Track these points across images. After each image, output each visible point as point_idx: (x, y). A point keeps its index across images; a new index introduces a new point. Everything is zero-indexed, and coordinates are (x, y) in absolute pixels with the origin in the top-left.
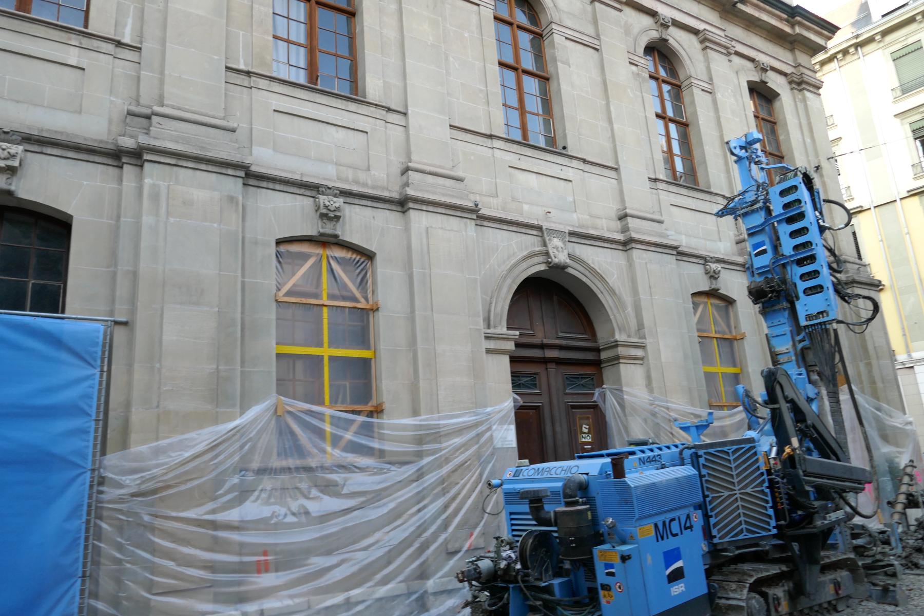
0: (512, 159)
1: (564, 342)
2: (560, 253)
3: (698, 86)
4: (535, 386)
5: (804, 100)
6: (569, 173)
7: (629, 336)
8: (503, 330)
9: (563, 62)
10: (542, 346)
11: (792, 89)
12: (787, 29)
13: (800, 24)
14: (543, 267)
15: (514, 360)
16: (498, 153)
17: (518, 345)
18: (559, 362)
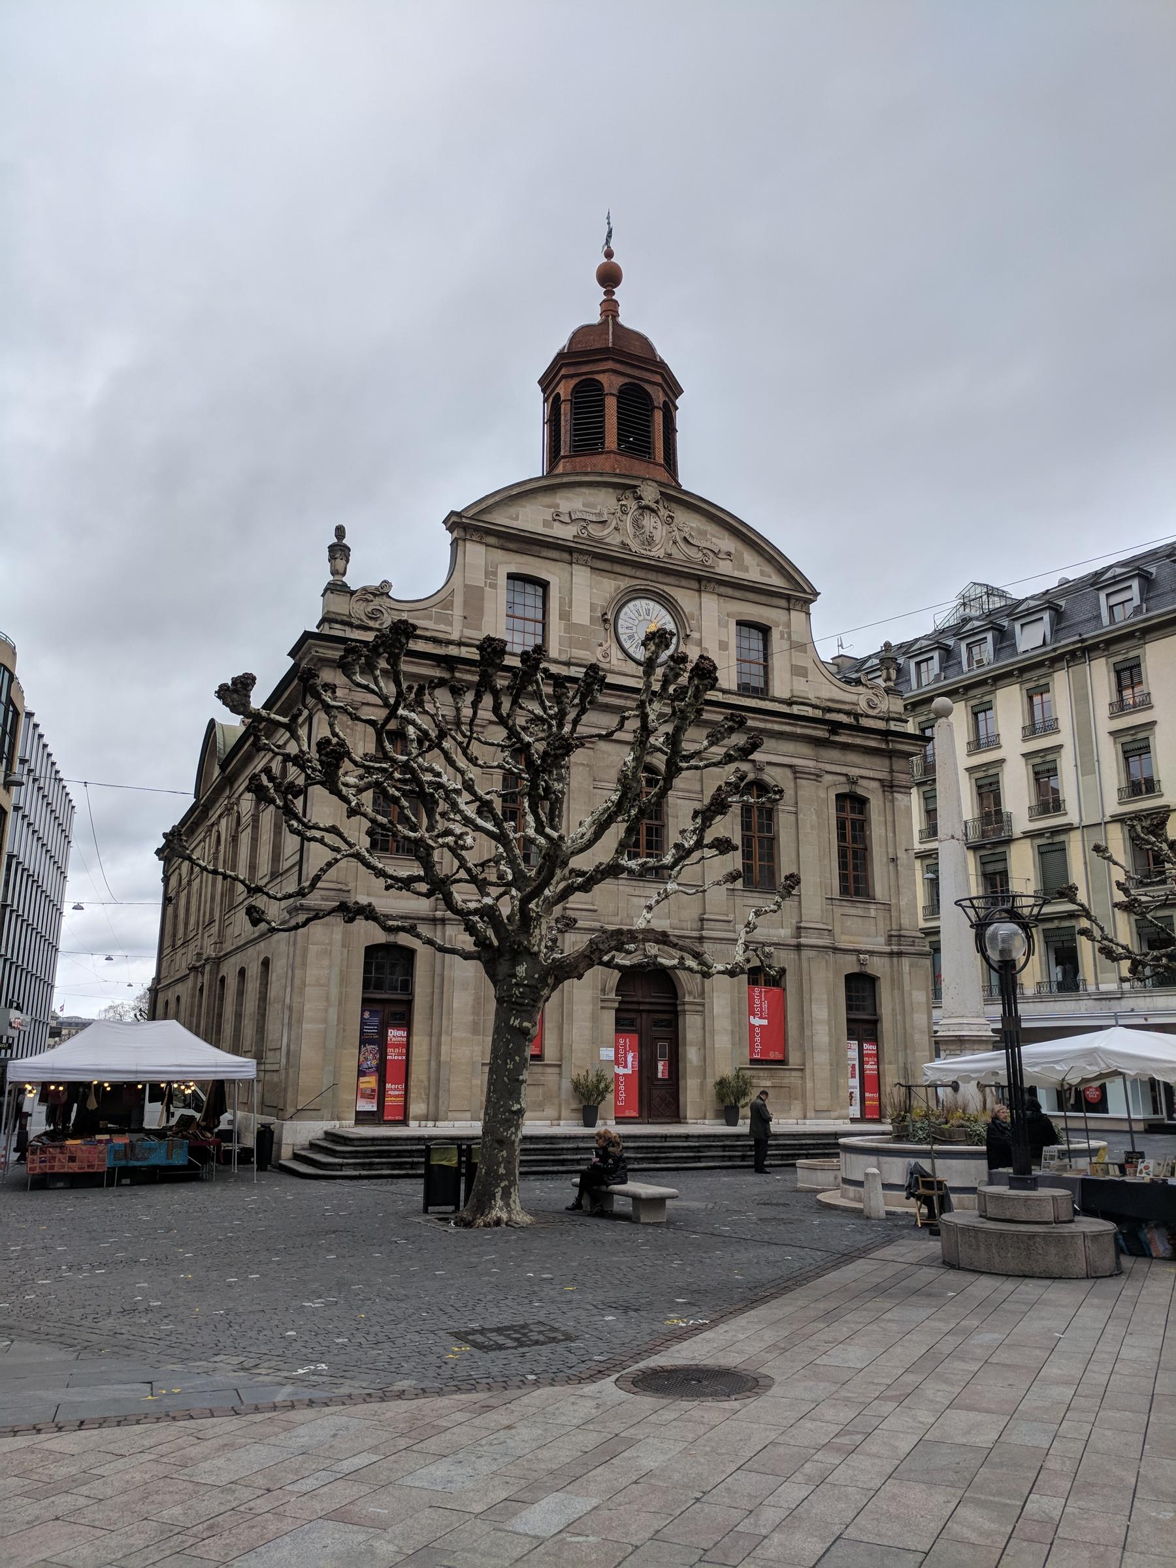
0: (629, 890)
1: (653, 1000)
3: (783, 811)
4: (633, 1025)
5: (892, 801)
7: (695, 998)
8: (613, 996)
9: (673, 817)
10: (639, 1003)
11: (884, 791)
12: (884, 746)
13: (893, 741)
15: (618, 1010)
16: (621, 888)
17: (620, 1003)
18: (649, 1011)
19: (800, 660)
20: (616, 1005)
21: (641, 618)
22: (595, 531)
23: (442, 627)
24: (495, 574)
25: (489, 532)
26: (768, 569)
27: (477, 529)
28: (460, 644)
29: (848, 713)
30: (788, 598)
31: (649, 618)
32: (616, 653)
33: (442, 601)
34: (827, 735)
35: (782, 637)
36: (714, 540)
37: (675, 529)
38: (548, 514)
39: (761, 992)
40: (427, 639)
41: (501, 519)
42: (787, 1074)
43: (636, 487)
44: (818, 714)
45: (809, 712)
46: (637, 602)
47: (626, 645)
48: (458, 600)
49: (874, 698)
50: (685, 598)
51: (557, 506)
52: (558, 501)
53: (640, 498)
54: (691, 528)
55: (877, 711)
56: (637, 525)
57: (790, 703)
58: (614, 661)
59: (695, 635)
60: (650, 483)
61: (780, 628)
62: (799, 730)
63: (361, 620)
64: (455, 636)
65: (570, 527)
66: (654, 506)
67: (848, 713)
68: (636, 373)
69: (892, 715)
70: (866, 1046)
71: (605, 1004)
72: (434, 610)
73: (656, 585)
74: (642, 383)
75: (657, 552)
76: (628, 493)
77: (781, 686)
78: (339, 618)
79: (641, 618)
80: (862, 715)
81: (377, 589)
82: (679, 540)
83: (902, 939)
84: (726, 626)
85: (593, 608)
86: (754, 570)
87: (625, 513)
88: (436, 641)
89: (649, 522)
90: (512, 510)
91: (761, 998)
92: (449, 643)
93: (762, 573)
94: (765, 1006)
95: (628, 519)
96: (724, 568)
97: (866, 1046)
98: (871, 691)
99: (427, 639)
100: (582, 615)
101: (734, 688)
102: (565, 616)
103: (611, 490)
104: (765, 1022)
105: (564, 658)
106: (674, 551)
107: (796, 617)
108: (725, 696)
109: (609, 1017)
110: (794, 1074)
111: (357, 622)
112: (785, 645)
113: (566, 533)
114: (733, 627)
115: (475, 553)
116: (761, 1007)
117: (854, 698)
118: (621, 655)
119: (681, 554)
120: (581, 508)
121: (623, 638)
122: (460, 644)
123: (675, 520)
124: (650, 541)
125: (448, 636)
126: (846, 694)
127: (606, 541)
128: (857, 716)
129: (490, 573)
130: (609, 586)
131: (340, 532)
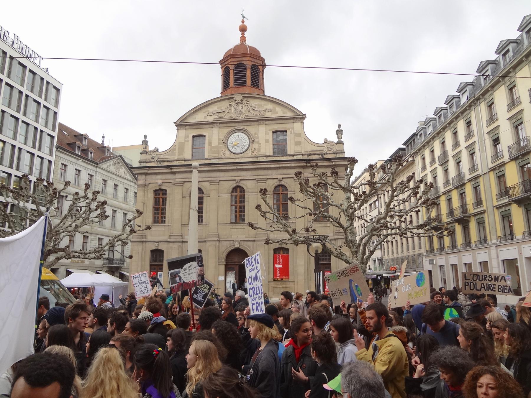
0: (231, 227)
2: (237, 245)
6: (244, 227)
14: (234, 248)
16: (228, 227)
17: (227, 262)
19: (298, 139)
20: (224, 263)
21: (236, 139)
22: (221, 115)
23: (173, 157)
24: (188, 137)
25: (186, 125)
26: (286, 110)
27: (182, 125)
28: (177, 160)
29: (318, 154)
30: (293, 119)
31: (239, 138)
32: (227, 152)
33: (173, 149)
34: (305, 164)
35: (291, 133)
36: (264, 106)
37: (249, 107)
38: (206, 114)
39: (280, 256)
40: (167, 161)
41: (191, 120)
42: (288, 283)
43: (234, 97)
44: (306, 157)
45: (301, 157)
46: (235, 134)
47: (230, 149)
48: (177, 148)
49: (331, 147)
50: (251, 129)
51: (209, 111)
52: (209, 109)
53: (236, 100)
54: (255, 105)
55: (332, 151)
56: (236, 109)
57: (293, 156)
58: (226, 155)
59: (256, 140)
60: (238, 95)
61: (291, 130)
62: (293, 165)
63: (149, 160)
64: (176, 159)
65: (213, 116)
66: (240, 102)
67: (318, 154)
68: (238, 59)
69: (338, 151)
70: (326, 273)
71: (220, 263)
72: (170, 152)
73: (240, 127)
74: (242, 62)
75: (242, 116)
76: (232, 100)
77: (291, 150)
78: (142, 161)
79: (236, 139)
80: (324, 154)
81: (153, 150)
82: (250, 110)
83: (339, 233)
84: (268, 134)
85: (219, 139)
86: (280, 112)
87: (231, 107)
88: (169, 161)
89: (239, 107)
90: (194, 116)
91: (280, 258)
92: (173, 161)
93: (284, 113)
94: (281, 261)
95: (232, 108)
96: (269, 115)
97: (326, 273)
98: (330, 144)
99: (167, 161)
100: (215, 143)
101: (271, 154)
102: (210, 144)
103: (227, 101)
104: (281, 266)
105: (210, 157)
106: (249, 114)
107: (297, 125)
108: (267, 158)
109: (222, 268)
110: (291, 283)
111: (148, 161)
112: (293, 135)
113: (210, 119)
114: (271, 134)
115: (182, 132)
116: (280, 261)
117: (322, 148)
118: (228, 152)
119: (252, 115)
120: (217, 109)
121: (229, 147)
122: (177, 160)
123: (249, 104)
124: (241, 113)
125: (173, 159)
126: (318, 147)
127: (225, 117)
128: (322, 154)
129: (186, 137)
130: (226, 131)
131: (145, 137)
